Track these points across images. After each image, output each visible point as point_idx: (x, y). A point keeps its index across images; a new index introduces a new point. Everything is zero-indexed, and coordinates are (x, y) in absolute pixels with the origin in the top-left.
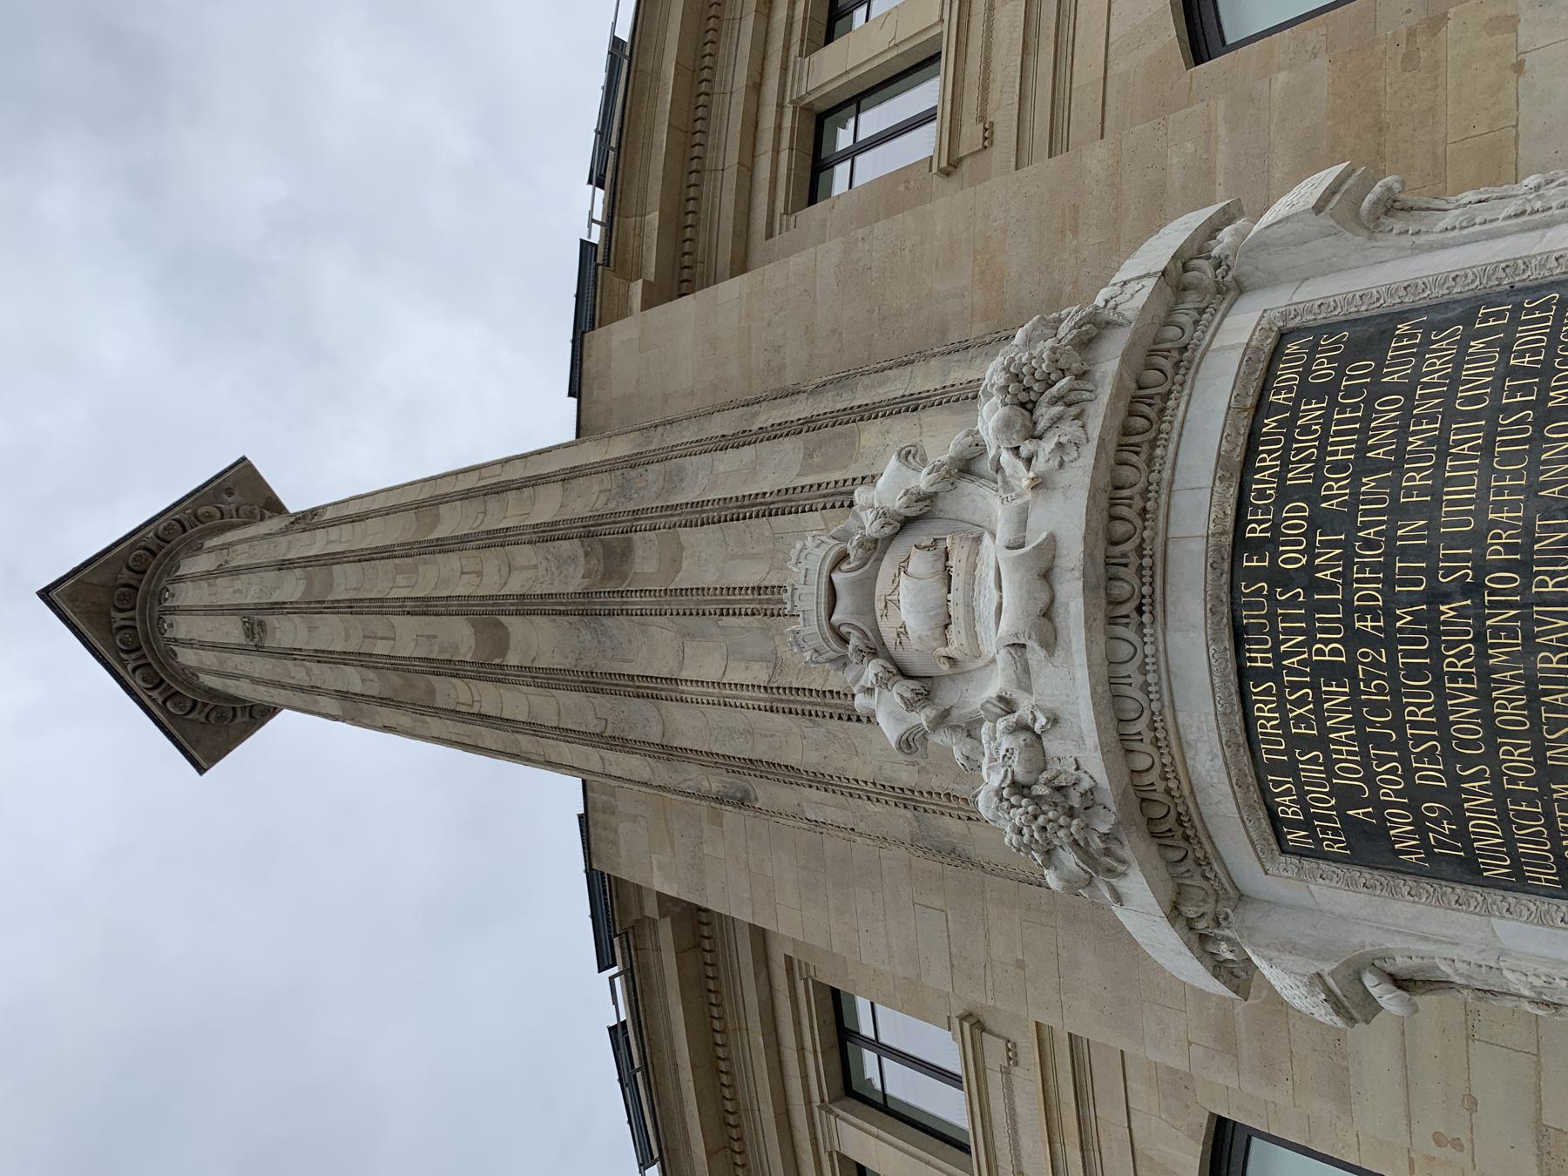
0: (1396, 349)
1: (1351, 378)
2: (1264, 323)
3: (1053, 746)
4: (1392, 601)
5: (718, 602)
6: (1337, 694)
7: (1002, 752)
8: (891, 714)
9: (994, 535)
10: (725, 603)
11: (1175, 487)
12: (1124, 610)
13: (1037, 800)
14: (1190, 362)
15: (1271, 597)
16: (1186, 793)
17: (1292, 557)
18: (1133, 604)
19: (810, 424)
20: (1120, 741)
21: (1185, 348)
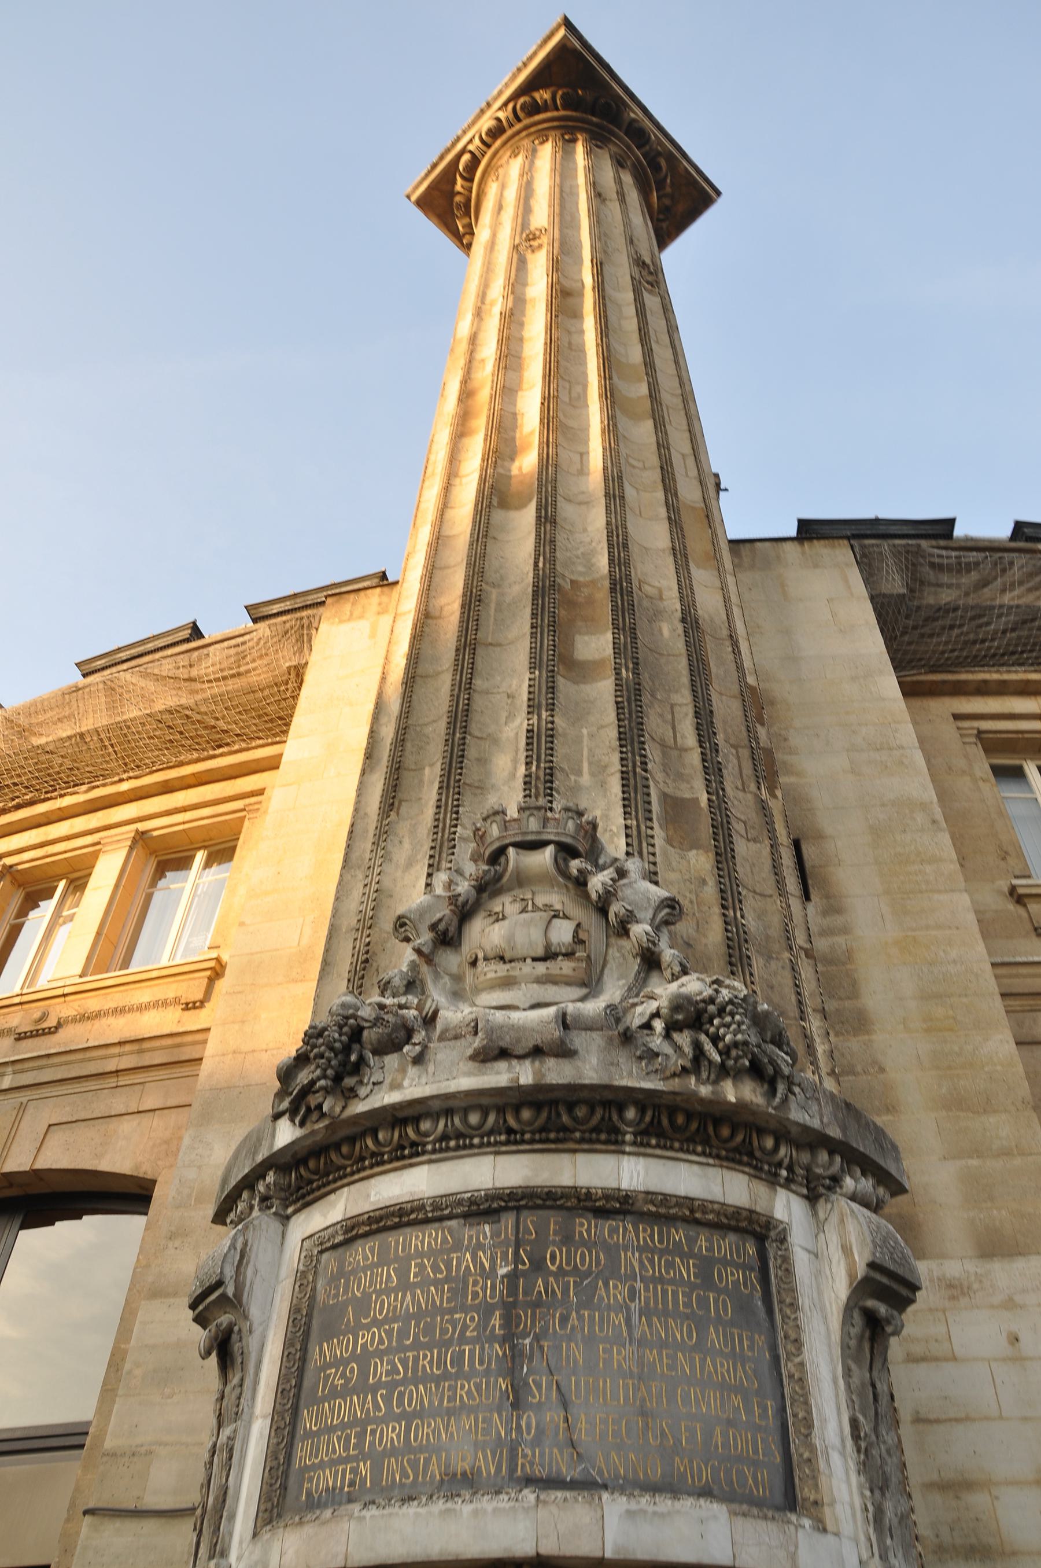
1: (716, 1301)
3: (392, 1060)
9: (583, 999)
13: (347, 1050)
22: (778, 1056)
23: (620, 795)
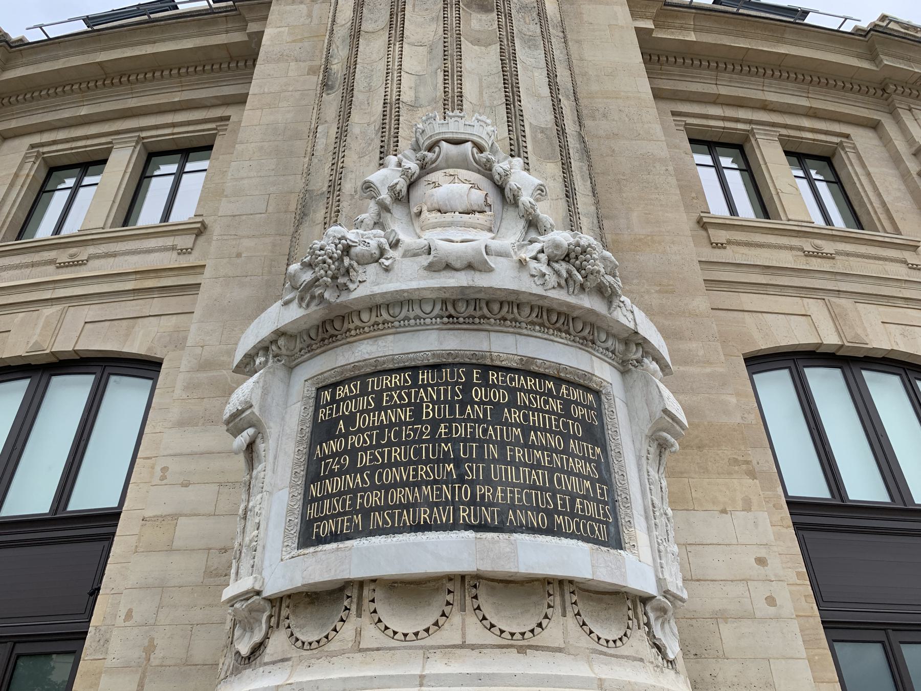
0: (587, 447)
2: (604, 384)
4: (455, 442)
5: (453, 69)
6: (405, 415)
7: (367, 241)
8: (387, 177)
10: (452, 74)
11: (518, 336)
12: (450, 308)
13: (340, 259)
14: (586, 345)
15: (457, 383)
16: (348, 340)
17: (478, 394)
18: (453, 312)
19: (561, 132)
20: (376, 305)
21: (593, 343)
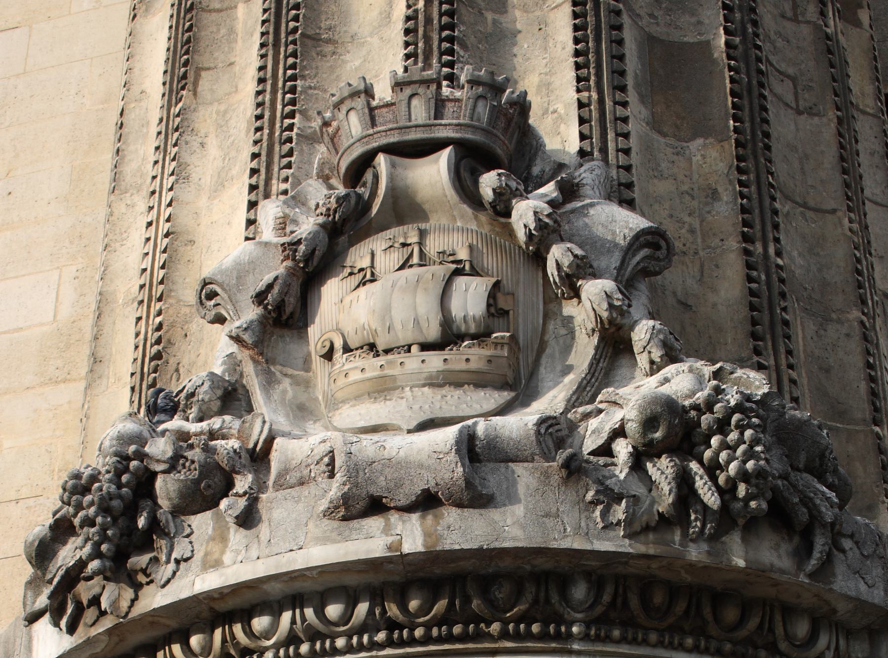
3: (201, 523)
9: (502, 411)
22: (816, 492)
23: (570, 47)
